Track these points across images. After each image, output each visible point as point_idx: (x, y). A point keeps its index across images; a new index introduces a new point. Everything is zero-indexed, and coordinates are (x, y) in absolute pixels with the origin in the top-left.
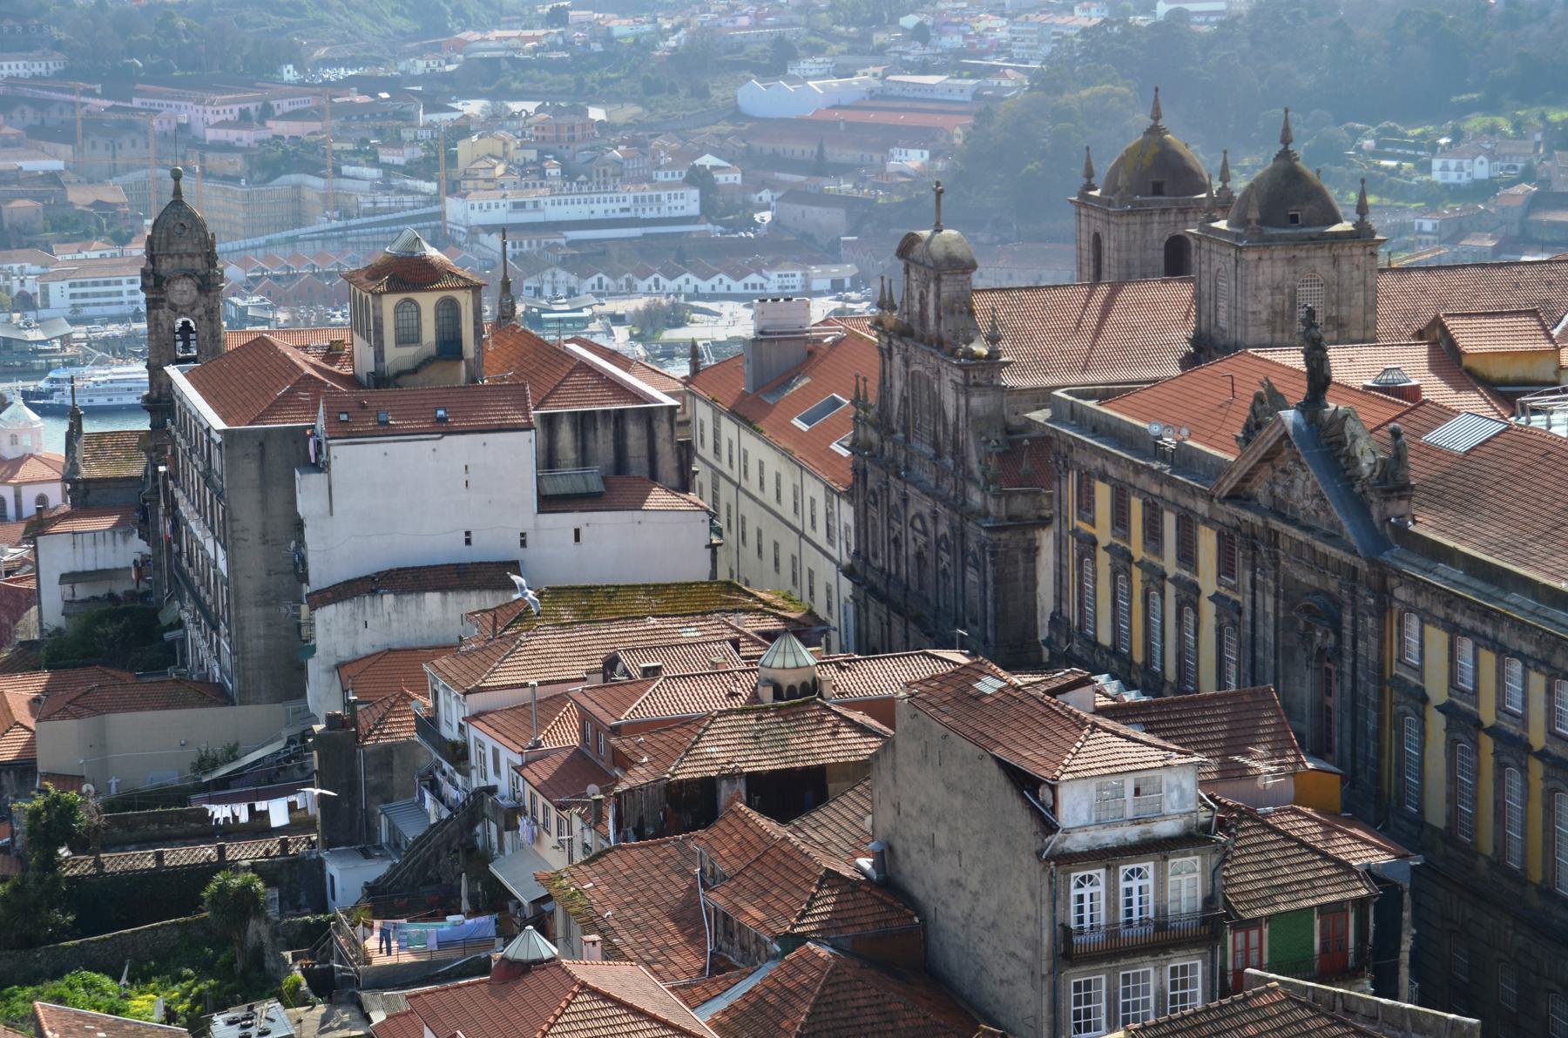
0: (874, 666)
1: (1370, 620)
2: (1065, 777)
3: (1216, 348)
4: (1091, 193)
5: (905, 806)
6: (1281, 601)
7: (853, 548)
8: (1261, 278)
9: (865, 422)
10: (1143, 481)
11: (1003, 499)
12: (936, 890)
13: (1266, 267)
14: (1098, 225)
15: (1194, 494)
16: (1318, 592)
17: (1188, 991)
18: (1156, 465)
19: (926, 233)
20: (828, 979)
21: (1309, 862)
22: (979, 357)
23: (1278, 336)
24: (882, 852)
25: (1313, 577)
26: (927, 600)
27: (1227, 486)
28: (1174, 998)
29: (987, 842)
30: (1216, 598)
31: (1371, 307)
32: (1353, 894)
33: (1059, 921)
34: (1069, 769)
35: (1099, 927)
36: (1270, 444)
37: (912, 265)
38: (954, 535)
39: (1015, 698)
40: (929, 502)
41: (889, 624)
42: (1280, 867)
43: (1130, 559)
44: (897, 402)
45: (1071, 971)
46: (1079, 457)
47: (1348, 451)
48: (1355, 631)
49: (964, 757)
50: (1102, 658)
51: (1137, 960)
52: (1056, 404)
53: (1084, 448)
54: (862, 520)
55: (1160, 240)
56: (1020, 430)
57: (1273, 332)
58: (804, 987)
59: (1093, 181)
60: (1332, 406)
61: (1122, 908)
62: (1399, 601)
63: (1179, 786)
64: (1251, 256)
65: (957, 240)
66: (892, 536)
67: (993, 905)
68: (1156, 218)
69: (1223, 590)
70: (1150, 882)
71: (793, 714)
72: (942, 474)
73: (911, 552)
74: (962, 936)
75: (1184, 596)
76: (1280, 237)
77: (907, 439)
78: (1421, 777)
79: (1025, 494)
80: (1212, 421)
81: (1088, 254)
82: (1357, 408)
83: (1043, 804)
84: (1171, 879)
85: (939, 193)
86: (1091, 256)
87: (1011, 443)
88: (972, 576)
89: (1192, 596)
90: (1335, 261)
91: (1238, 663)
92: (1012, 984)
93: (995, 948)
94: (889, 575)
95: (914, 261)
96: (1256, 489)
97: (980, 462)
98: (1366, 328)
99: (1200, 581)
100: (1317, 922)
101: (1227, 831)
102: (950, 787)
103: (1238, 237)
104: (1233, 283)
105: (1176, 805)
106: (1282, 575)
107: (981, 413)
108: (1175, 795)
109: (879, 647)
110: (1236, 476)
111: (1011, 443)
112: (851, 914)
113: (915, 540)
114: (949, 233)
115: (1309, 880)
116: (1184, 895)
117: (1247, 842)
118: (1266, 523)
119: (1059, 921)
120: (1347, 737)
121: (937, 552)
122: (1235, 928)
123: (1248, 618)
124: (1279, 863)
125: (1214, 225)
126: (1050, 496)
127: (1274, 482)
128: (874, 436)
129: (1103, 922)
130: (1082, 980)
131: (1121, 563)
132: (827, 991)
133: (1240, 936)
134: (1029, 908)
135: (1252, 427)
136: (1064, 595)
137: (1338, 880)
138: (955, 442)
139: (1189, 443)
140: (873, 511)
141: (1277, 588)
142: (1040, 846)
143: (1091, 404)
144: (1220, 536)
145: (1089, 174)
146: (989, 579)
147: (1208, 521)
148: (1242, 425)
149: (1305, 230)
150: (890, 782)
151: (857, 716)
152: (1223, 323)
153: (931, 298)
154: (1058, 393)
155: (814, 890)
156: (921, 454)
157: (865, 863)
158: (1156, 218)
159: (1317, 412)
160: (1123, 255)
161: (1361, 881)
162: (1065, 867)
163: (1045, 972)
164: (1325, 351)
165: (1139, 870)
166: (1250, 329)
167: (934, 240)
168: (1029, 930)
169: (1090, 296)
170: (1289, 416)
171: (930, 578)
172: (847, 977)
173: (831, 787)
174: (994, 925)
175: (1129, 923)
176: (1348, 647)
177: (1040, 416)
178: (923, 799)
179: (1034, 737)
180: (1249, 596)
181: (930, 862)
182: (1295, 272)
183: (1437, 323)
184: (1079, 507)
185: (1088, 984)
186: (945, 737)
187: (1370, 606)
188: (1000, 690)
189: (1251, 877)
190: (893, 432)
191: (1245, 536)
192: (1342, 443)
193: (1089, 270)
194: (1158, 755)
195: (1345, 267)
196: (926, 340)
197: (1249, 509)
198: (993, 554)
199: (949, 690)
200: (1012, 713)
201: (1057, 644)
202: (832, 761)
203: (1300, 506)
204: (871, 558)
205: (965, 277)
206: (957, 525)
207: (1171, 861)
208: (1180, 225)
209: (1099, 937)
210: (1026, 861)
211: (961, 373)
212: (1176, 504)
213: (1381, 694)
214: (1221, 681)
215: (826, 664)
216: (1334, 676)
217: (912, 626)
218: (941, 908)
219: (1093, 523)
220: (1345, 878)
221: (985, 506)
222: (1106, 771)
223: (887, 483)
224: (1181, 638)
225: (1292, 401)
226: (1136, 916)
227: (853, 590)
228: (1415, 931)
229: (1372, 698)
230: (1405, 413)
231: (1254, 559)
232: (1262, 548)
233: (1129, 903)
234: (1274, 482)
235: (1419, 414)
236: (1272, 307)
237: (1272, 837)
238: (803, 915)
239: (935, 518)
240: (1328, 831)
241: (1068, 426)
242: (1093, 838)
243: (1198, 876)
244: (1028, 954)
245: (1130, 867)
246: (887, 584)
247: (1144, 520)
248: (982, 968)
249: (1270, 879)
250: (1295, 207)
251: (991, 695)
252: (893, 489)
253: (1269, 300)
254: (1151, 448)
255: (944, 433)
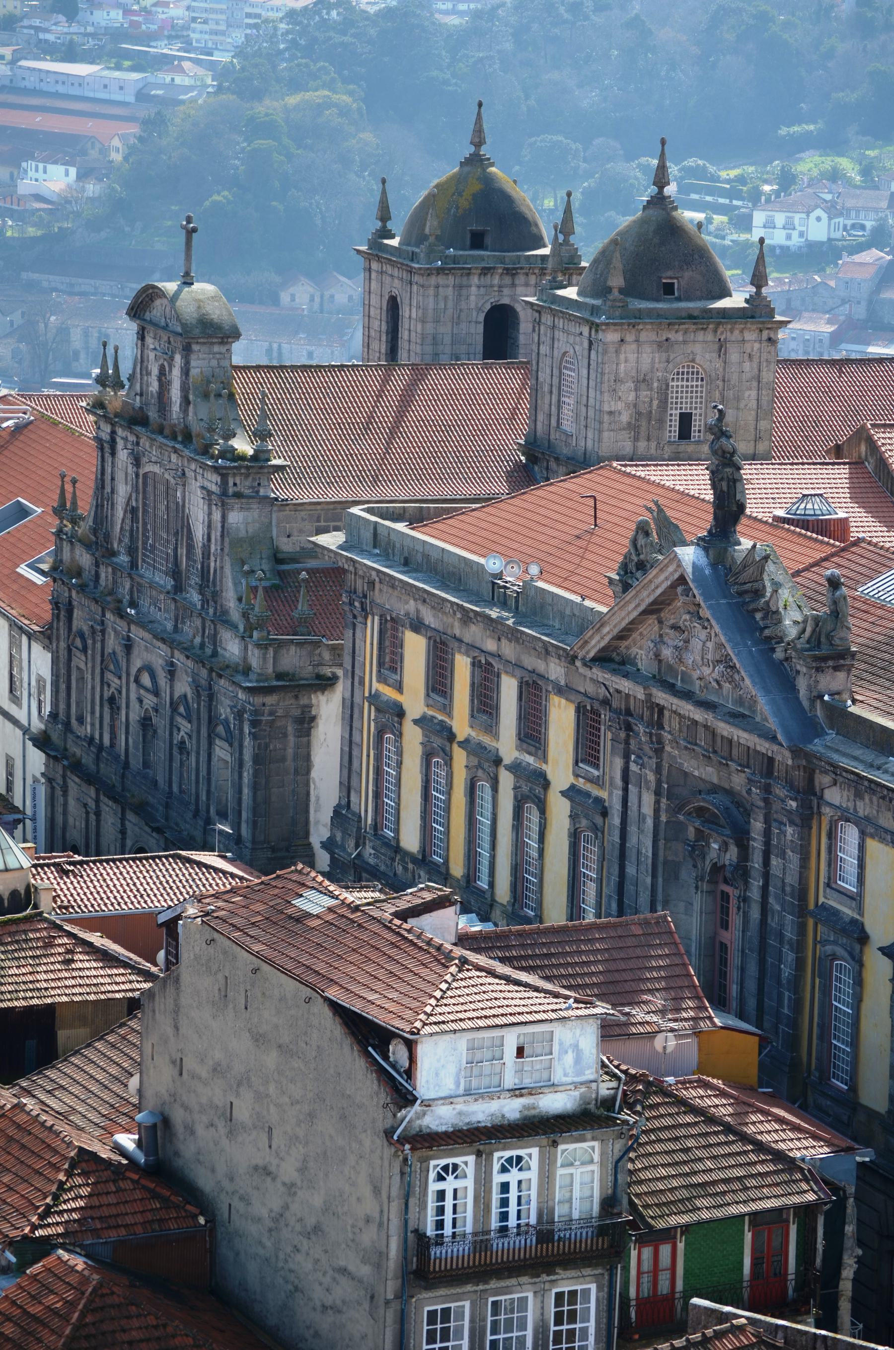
0: (108, 871)
1: (790, 830)
2: (427, 1030)
3: (557, 459)
4: (386, 241)
5: (190, 1063)
6: (664, 800)
7: (47, 709)
8: (622, 367)
9: (72, 539)
10: (474, 633)
11: (271, 651)
12: (232, 1179)
13: (629, 352)
14: (396, 287)
15: (547, 653)
16: (714, 789)
17: (578, 1326)
18: (494, 613)
19: (171, 287)
20: (90, 1301)
21: (738, 1154)
22: (242, 458)
23: (642, 445)
24: (154, 1126)
25: (710, 769)
26: (155, 783)
27: (596, 644)
28: (558, 1334)
29: (311, 1116)
30: (571, 793)
31: (763, 411)
32: (796, 1200)
33: (411, 1227)
34: (433, 1019)
35: (464, 1235)
36: (659, 591)
37: (149, 327)
38: (199, 696)
39: (352, 921)
40: (163, 650)
41: (98, 814)
42: (700, 1160)
43: (451, 737)
44: (120, 513)
45: (425, 1295)
46: (382, 597)
47: (767, 603)
48: (767, 843)
49: (282, 999)
50: (406, 869)
51: (513, 1281)
52: (352, 526)
53: (393, 587)
54: (63, 671)
55: (479, 310)
56: (293, 559)
57: (636, 439)
58: (55, 1313)
59: (390, 225)
60: (746, 544)
61: (495, 1210)
62: (831, 805)
63: (576, 1047)
64: (611, 337)
65: (214, 298)
66: (107, 695)
67: (317, 1201)
68: (475, 280)
69: (581, 783)
70: (532, 1175)
71: (10, 934)
72: (182, 613)
73: (134, 717)
74: (268, 1244)
75: (525, 789)
76: (650, 313)
77: (134, 565)
78: (855, 1042)
79: (300, 644)
80: (567, 556)
81: (380, 325)
82: (779, 551)
83: (393, 1066)
84: (560, 1172)
85: (190, 232)
86: (384, 327)
87: (281, 575)
88: (222, 751)
89: (538, 790)
90: (721, 347)
91: (600, 881)
92: (339, 1312)
93: (317, 1261)
94: (101, 747)
95: (151, 322)
96: (634, 650)
97: (240, 600)
98: (757, 439)
99: (549, 770)
100: (748, 1236)
101: (631, 1107)
102: (259, 1039)
103: (594, 310)
104: (584, 372)
105: (570, 1071)
106: (666, 765)
107: (242, 534)
108: (569, 1058)
109: (81, 843)
110: (608, 632)
111: (281, 575)
112: (114, 1211)
113: (141, 701)
114: (203, 288)
115: (739, 1179)
116: (576, 1194)
117: (657, 1124)
118: (649, 696)
119: (411, 1227)
120: (751, 985)
121: (172, 719)
122: (642, 1242)
123: (617, 821)
124: (699, 1153)
125: (560, 292)
126: (333, 648)
127: (660, 640)
128: (85, 559)
129: (469, 1229)
130: (439, 1307)
131: (437, 742)
132: (89, 1319)
133: (647, 1252)
134: (370, 1206)
135: (632, 567)
136: (354, 783)
137: (777, 1179)
138: (204, 573)
139: (540, 584)
140: (79, 660)
141: (659, 782)
142: (389, 1123)
143: (401, 527)
144: (580, 710)
145: (385, 215)
146: (247, 756)
147: (561, 691)
148: (616, 566)
149: (683, 305)
150: (170, 1031)
151: (96, 939)
152: (568, 425)
153: (176, 374)
154: (355, 510)
155: (62, 1177)
156: (152, 585)
157: (127, 1141)
158: (475, 280)
159: (726, 550)
160: (430, 328)
161: (807, 1181)
162: (424, 1153)
163: (390, 1296)
164: (739, 468)
165: (519, 1159)
166: (606, 434)
167: (183, 295)
168: (368, 1237)
169: (385, 381)
170: (689, 555)
171: (160, 752)
172: (116, 1300)
173: (62, 1035)
174: (317, 1229)
175: (503, 1230)
176: (756, 862)
177: (331, 540)
178: (218, 1055)
179: (381, 974)
180: (618, 793)
181: (225, 1142)
182: (668, 362)
183: (862, 436)
184: (380, 664)
185: (446, 1312)
186: (255, 971)
187: (790, 812)
188: (330, 910)
189: (663, 1172)
190: (113, 554)
191: (618, 712)
192: (758, 593)
193: (380, 346)
194: (551, 1003)
195: (734, 356)
196: (167, 431)
197: (626, 676)
198: (254, 723)
199: (259, 907)
200: (349, 940)
201: (344, 849)
202: (65, 999)
203: (696, 674)
204: (74, 721)
205: (223, 349)
206: (203, 683)
207: (561, 1147)
208: (506, 291)
209: (463, 1249)
210: (367, 1143)
211: (216, 478)
212: (518, 666)
213: (802, 929)
214: (574, 907)
215: (42, 866)
216: (733, 903)
217: (131, 816)
218: (236, 1203)
219: (399, 688)
220: (785, 1177)
221: (245, 659)
222: (481, 1023)
223: (102, 623)
224: (519, 846)
225: (689, 538)
226: (512, 1222)
227: (47, 765)
228: (860, 1252)
229: (789, 934)
230: (833, 555)
231: (627, 742)
232: (641, 729)
233: (505, 1203)
234: (660, 640)
235: (850, 556)
236: (635, 405)
237: (689, 1119)
238: (48, 1212)
239: (172, 673)
240: (743, 1108)
241: (371, 556)
242: (460, 1113)
243: (595, 1168)
244: (365, 1271)
245: (507, 1154)
246: (98, 759)
247: (473, 685)
248: (296, 1289)
249: (687, 1175)
250: (669, 273)
251: (318, 916)
252: (109, 630)
253: (632, 396)
254: (486, 590)
255: (188, 558)
